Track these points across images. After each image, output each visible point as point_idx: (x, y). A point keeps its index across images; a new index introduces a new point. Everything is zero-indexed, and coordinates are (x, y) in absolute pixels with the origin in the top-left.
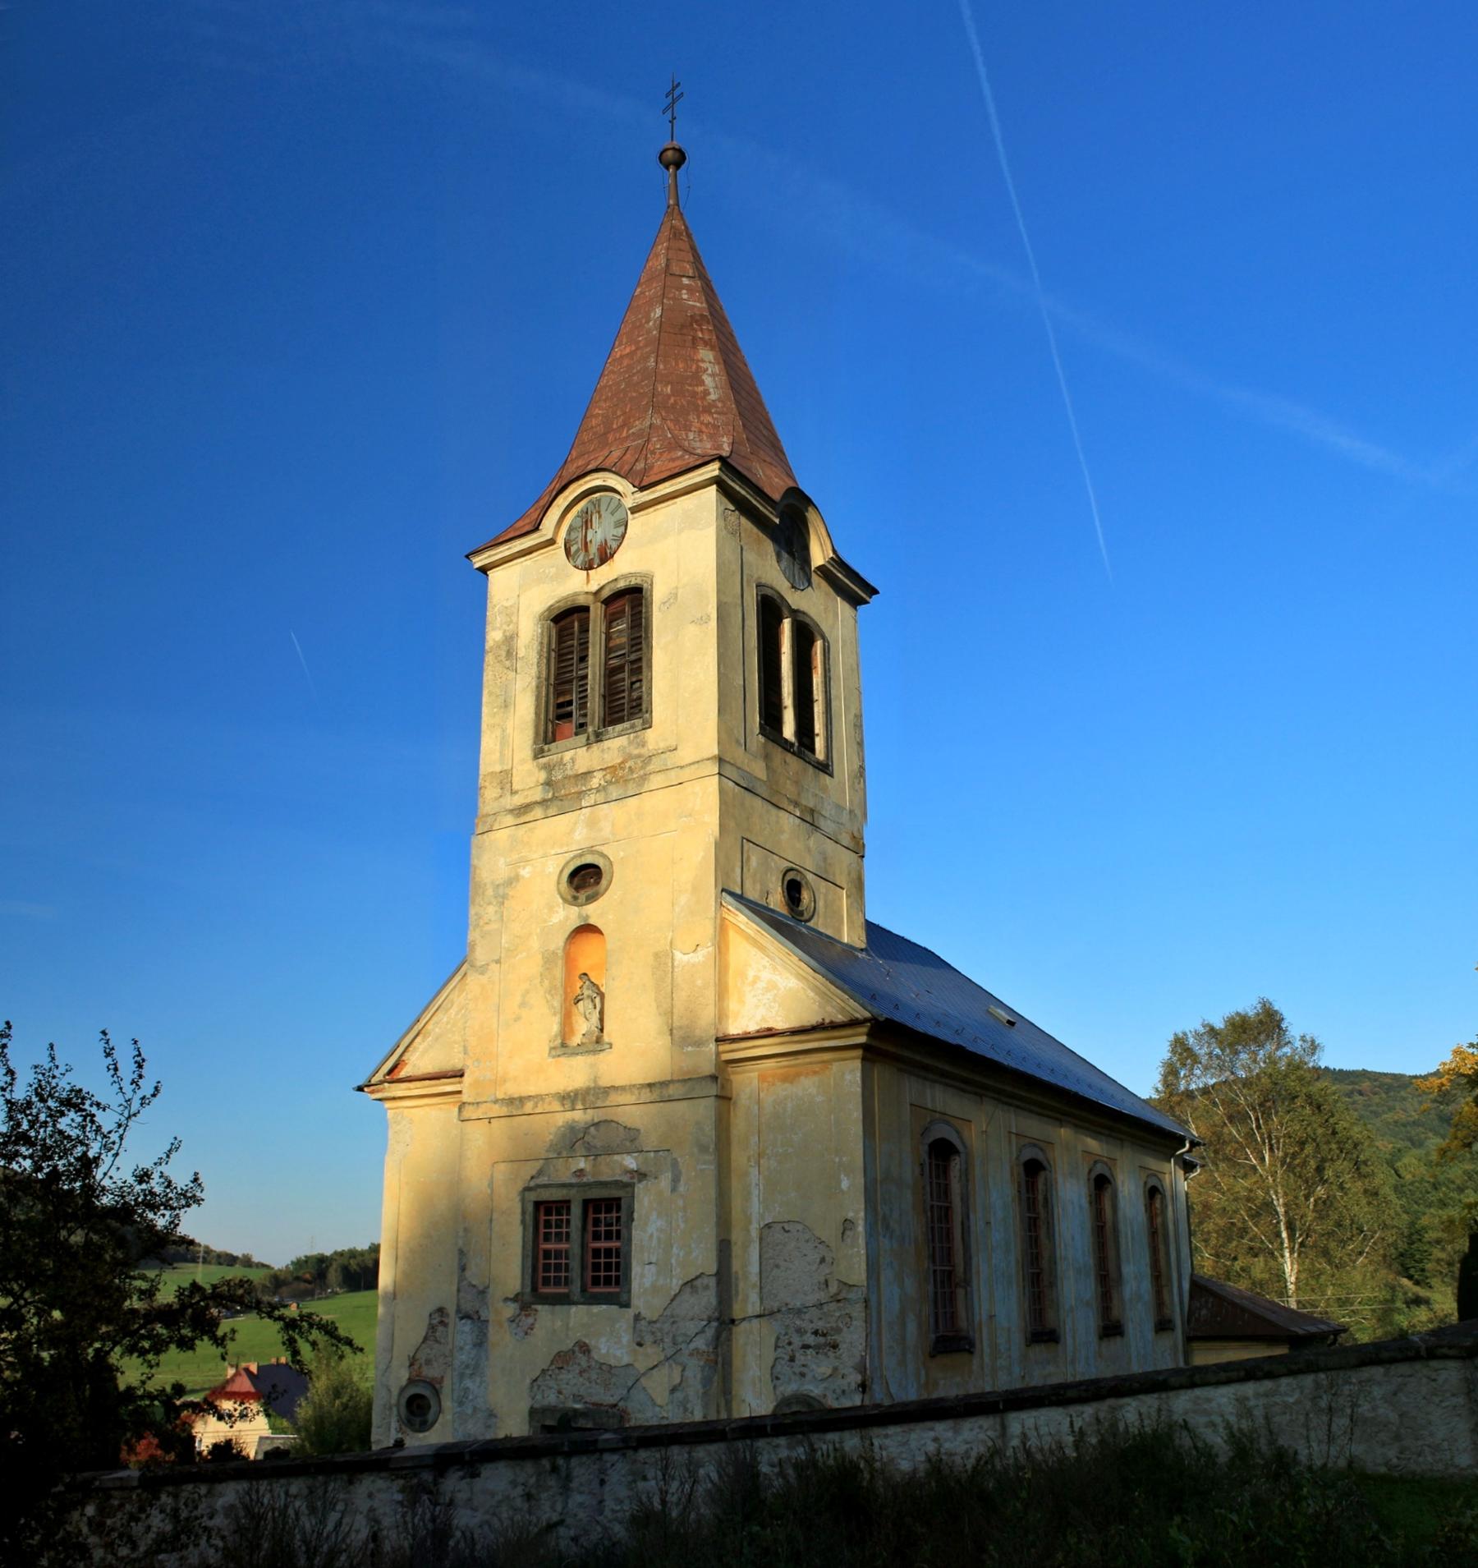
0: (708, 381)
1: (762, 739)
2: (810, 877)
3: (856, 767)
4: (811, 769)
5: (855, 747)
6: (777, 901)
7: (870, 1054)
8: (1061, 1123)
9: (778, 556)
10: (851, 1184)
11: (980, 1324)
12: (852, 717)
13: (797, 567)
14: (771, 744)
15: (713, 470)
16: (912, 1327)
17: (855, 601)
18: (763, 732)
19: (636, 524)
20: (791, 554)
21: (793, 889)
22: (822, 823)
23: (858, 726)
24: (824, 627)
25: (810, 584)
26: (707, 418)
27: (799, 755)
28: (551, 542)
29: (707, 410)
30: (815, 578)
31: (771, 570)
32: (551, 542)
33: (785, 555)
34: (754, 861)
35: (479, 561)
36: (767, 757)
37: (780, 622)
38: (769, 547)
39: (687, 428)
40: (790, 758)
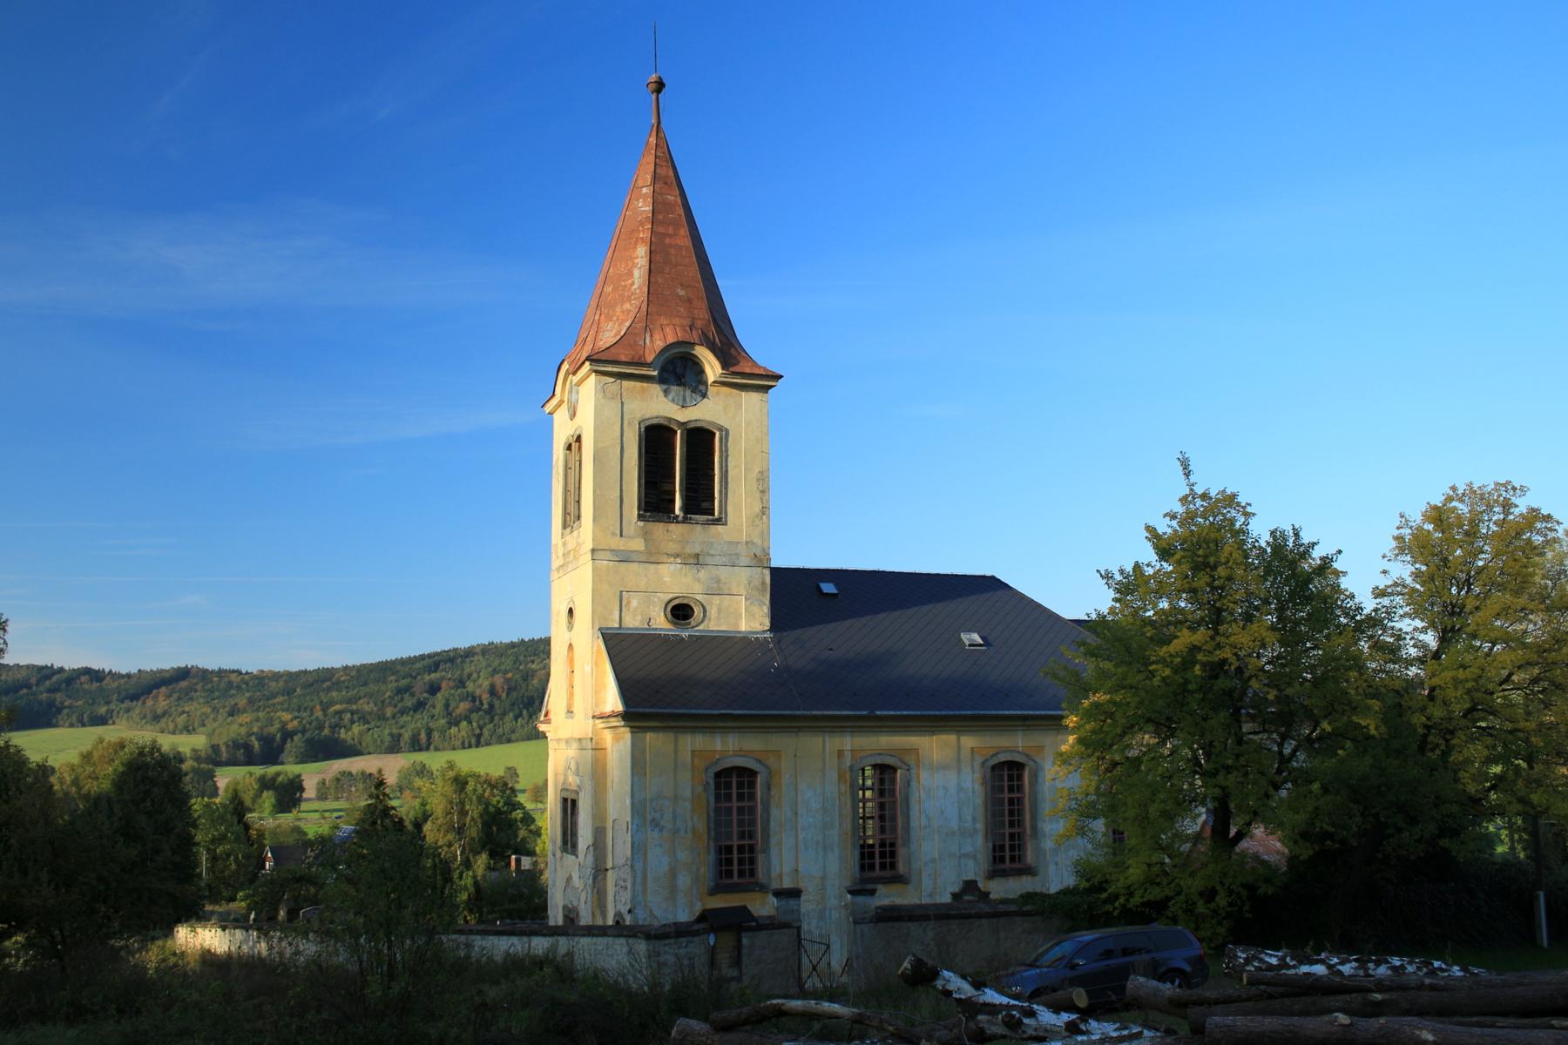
0: (636, 273)
1: (641, 524)
3: (757, 507)
5: (758, 495)
7: (635, 730)
9: (666, 392)
10: (628, 802)
12: (754, 475)
13: (688, 392)
16: (684, 881)
17: (766, 389)
18: (640, 517)
20: (680, 381)
21: (681, 612)
22: (708, 560)
23: (763, 478)
24: (721, 422)
25: (704, 396)
26: (627, 306)
27: (685, 520)
28: (562, 402)
29: (629, 299)
31: (658, 404)
32: (562, 402)
33: (674, 388)
34: (634, 603)
35: (548, 409)
36: (646, 535)
38: (656, 389)
40: (673, 527)
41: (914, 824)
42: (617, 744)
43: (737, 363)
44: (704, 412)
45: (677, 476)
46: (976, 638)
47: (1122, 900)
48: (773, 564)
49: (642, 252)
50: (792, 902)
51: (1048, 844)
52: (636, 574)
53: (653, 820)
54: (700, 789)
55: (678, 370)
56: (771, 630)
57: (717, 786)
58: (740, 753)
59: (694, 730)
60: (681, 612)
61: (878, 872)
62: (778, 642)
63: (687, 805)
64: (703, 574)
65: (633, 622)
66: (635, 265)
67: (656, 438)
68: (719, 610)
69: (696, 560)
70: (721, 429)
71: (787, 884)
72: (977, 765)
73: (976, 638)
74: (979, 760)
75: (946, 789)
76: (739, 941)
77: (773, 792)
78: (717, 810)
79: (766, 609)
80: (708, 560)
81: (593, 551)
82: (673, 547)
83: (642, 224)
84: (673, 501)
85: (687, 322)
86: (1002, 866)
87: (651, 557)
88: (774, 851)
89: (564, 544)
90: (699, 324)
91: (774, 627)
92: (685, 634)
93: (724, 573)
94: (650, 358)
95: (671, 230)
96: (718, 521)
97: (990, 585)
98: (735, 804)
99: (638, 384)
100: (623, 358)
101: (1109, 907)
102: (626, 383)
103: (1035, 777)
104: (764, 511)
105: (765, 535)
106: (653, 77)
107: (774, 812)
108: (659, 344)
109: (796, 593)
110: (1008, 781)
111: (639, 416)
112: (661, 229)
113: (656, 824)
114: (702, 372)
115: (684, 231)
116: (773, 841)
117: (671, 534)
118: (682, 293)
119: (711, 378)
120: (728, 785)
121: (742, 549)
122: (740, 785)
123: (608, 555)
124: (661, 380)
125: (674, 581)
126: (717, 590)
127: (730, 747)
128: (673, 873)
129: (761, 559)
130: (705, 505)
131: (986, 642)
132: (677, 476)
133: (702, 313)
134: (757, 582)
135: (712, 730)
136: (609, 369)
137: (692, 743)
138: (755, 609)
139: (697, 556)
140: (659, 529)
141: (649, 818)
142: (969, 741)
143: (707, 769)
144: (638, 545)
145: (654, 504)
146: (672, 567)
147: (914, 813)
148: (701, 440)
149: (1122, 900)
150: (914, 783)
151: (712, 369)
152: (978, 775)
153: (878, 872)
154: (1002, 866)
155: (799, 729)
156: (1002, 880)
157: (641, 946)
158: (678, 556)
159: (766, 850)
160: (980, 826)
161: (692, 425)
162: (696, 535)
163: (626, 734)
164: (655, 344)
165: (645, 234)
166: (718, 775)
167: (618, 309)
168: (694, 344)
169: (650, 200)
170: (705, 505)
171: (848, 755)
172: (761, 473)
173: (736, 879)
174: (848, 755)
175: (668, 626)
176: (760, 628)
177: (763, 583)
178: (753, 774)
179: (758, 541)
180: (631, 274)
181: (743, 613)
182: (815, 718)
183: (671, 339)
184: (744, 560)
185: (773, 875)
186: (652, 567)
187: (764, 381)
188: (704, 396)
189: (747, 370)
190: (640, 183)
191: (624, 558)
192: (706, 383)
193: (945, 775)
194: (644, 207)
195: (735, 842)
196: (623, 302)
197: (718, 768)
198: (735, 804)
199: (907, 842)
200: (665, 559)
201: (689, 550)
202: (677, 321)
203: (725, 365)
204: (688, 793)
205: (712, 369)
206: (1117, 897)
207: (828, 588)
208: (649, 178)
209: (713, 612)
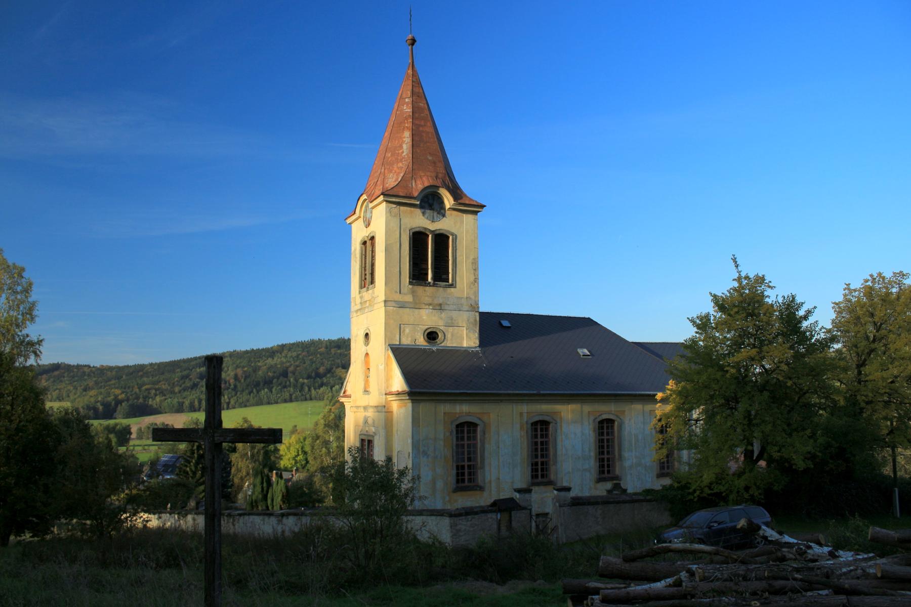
0: (405, 146)
2: (442, 328)
3: (472, 278)
4: (441, 289)
5: (472, 271)
6: (421, 341)
7: (413, 401)
8: (569, 403)
9: (424, 213)
10: (410, 441)
11: (490, 482)
12: (470, 260)
13: (435, 214)
14: (416, 287)
15: (381, 198)
16: (440, 484)
17: (476, 213)
18: (410, 283)
19: (374, 211)
20: (431, 207)
21: (432, 336)
22: (446, 307)
23: (475, 262)
24: (453, 231)
25: (444, 216)
26: (400, 165)
27: (434, 285)
28: (360, 217)
29: (401, 161)
30: (448, 213)
31: (419, 220)
32: (360, 217)
33: (428, 211)
34: (407, 331)
35: (348, 221)
36: (413, 293)
37: (428, 236)
38: (418, 212)
39: (391, 171)
40: (427, 288)
41: (559, 453)
42: (401, 410)
43: (461, 198)
44: (443, 225)
45: (429, 260)
46: (586, 351)
47: (698, 493)
48: (481, 310)
49: (407, 134)
50: (527, 496)
51: (627, 464)
52: (408, 315)
53: (424, 451)
54: (448, 434)
55: (430, 202)
56: (479, 346)
57: (457, 431)
58: (469, 414)
59: (445, 401)
60: (432, 336)
61: (540, 479)
62: (484, 353)
63: (442, 443)
64: (443, 315)
65: (406, 341)
66: (403, 142)
67: (418, 239)
68: (452, 335)
69: (440, 307)
70: (452, 234)
71: (565, 484)
72: (591, 421)
73: (586, 351)
74: (592, 418)
75: (575, 434)
76: (510, 516)
77: (487, 436)
78: (457, 445)
79: (477, 335)
80: (446, 307)
81: (385, 301)
82: (427, 300)
83: (407, 119)
84: (427, 274)
85: (434, 174)
86: (603, 476)
87: (416, 305)
88: (487, 468)
89: (361, 297)
90: (440, 176)
91: (481, 345)
92: (434, 348)
93: (455, 314)
94: (416, 194)
95: (422, 123)
96: (452, 286)
97: (587, 322)
98: (466, 442)
99: (409, 209)
100: (401, 194)
101: (691, 497)
102: (402, 208)
103: (620, 426)
104: (476, 280)
105: (476, 294)
106: (410, 37)
107: (487, 446)
108: (420, 187)
109: (493, 326)
110: (606, 430)
111: (409, 227)
112: (417, 122)
113: (425, 453)
114: (442, 202)
115: (429, 124)
116: (486, 462)
117: (426, 293)
118: (430, 158)
119: (448, 206)
120: (463, 432)
121: (464, 301)
122: (469, 432)
123: (394, 304)
124: (421, 207)
125: (428, 318)
126: (451, 324)
127: (465, 410)
128: (434, 481)
129: (474, 307)
130: (444, 276)
131: (592, 355)
132: (429, 260)
133: (441, 170)
134: (472, 320)
135: (455, 401)
136: (394, 200)
137: (445, 408)
138: (471, 335)
139: (440, 305)
140: (420, 290)
141: (421, 450)
142: (587, 408)
143: (452, 423)
144: (409, 298)
145: (418, 276)
146: (427, 311)
147: (559, 447)
148: (442, 240)
149: (698, 493)
150: (559, 431)
151: (448, 201)
152: (591, 427)
153: (540, 479)
154: (603, 476)
155: (501, 401)
156: (604, 483)
157: (446, 521)
158: (430, 304)
159: (483, 467)
160: (592, 454)
161: (438, 232)
162: (439, 293)
163: (409, 405)
164: (418, 186)
165: (409, 124)
166: (457, 426)
167: (395, 166)
168: (438, 187)
169: (410, 105)
170: (444, 276)
171: (525, 415)
172: (474, 259)
173: (466, 483)
174: (525, 415)
175: (426, 344)
176: (473, 345)
177: (475, 320)
178: (475, 425)
179: (473, 297)
180: (401, 147)
181: (464, 337)
182: (509, 395)
183: (427, 184)
184: (466, 308)
185: (487, 481)
186: (417, 311)
187: (475, 208)
188: (444, 216)
189: (467, 202)
190: (404, 96)
191: (402, 305)
192: (444, 209)
193: (574, 427)
194: (407, 109)
195: (466, 463)
196: (398, 163)
197: (458, 422)
198: (466, 442)
199: (555, 463)
200: (423, 306)
201: (436, 302)
202: (429, 174)
203: (455, 199)
204: (442, 436)
205: (448, 201)
206: (695, 491)
207: (506, 323)
208: (409, 93)
209: (449, 336)
